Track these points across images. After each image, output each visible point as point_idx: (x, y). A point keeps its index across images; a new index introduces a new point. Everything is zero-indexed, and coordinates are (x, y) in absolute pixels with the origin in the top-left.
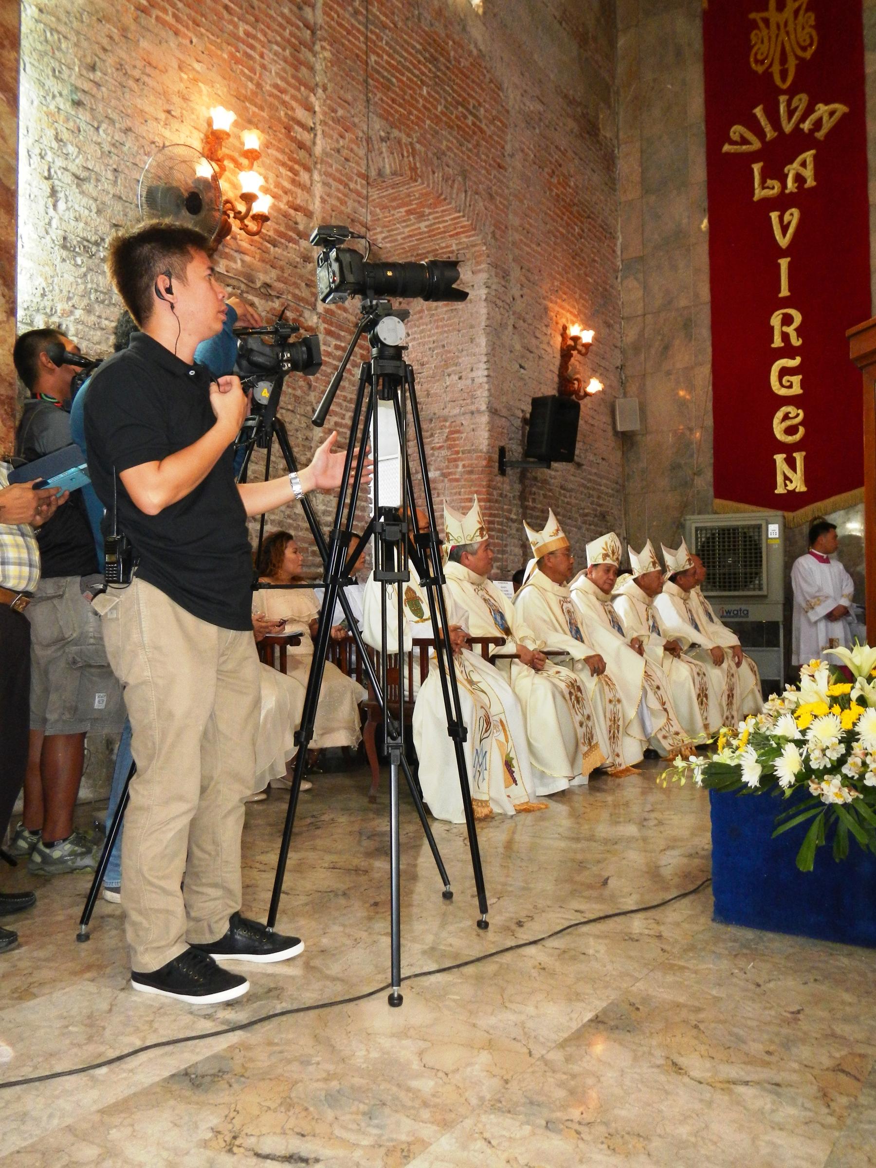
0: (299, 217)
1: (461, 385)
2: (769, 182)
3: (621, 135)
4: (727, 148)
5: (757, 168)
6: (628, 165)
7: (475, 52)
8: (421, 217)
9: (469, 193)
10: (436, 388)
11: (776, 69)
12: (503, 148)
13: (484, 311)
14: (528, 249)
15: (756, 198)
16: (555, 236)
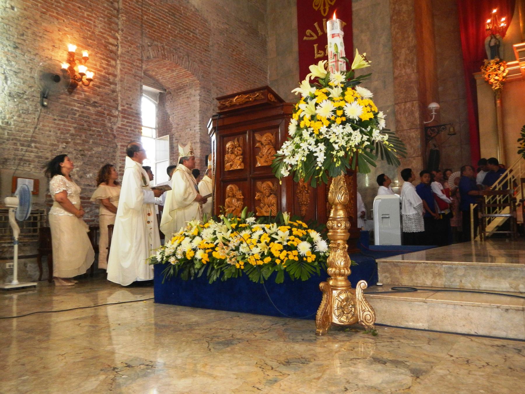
0: (111, 77)
1: (191, 132)
2: (320, 52)
3: (269, 33)
4: (305, 38)
5: (315, 46)
6: (271, 45)
7: (193, 10)
8: (173, 71)
9: (191, 62)
10: (183, 134)
11: (322, 8)
12: (208, 43)
13: (198, 105)
14: (221, 80)
15: (315, 58)
16: (235, 75)
